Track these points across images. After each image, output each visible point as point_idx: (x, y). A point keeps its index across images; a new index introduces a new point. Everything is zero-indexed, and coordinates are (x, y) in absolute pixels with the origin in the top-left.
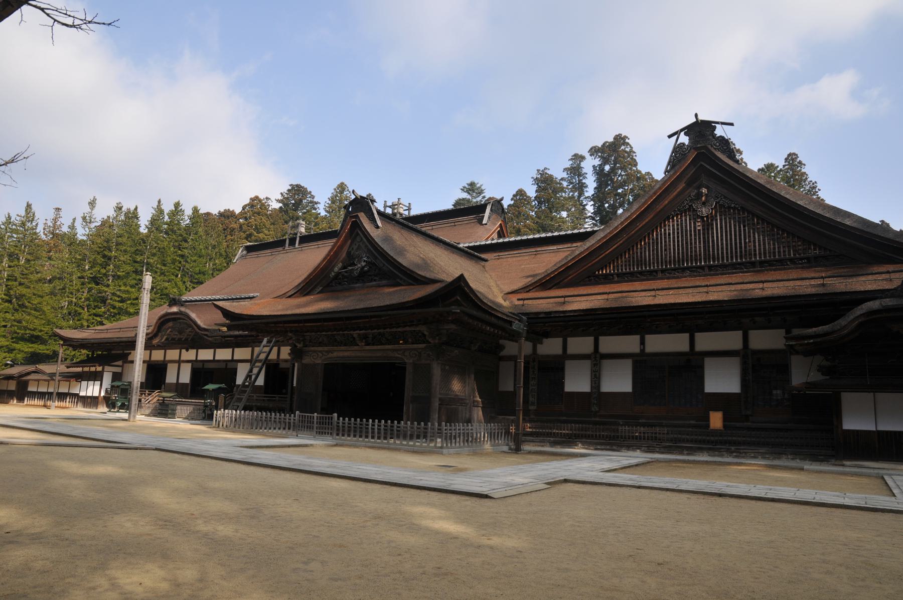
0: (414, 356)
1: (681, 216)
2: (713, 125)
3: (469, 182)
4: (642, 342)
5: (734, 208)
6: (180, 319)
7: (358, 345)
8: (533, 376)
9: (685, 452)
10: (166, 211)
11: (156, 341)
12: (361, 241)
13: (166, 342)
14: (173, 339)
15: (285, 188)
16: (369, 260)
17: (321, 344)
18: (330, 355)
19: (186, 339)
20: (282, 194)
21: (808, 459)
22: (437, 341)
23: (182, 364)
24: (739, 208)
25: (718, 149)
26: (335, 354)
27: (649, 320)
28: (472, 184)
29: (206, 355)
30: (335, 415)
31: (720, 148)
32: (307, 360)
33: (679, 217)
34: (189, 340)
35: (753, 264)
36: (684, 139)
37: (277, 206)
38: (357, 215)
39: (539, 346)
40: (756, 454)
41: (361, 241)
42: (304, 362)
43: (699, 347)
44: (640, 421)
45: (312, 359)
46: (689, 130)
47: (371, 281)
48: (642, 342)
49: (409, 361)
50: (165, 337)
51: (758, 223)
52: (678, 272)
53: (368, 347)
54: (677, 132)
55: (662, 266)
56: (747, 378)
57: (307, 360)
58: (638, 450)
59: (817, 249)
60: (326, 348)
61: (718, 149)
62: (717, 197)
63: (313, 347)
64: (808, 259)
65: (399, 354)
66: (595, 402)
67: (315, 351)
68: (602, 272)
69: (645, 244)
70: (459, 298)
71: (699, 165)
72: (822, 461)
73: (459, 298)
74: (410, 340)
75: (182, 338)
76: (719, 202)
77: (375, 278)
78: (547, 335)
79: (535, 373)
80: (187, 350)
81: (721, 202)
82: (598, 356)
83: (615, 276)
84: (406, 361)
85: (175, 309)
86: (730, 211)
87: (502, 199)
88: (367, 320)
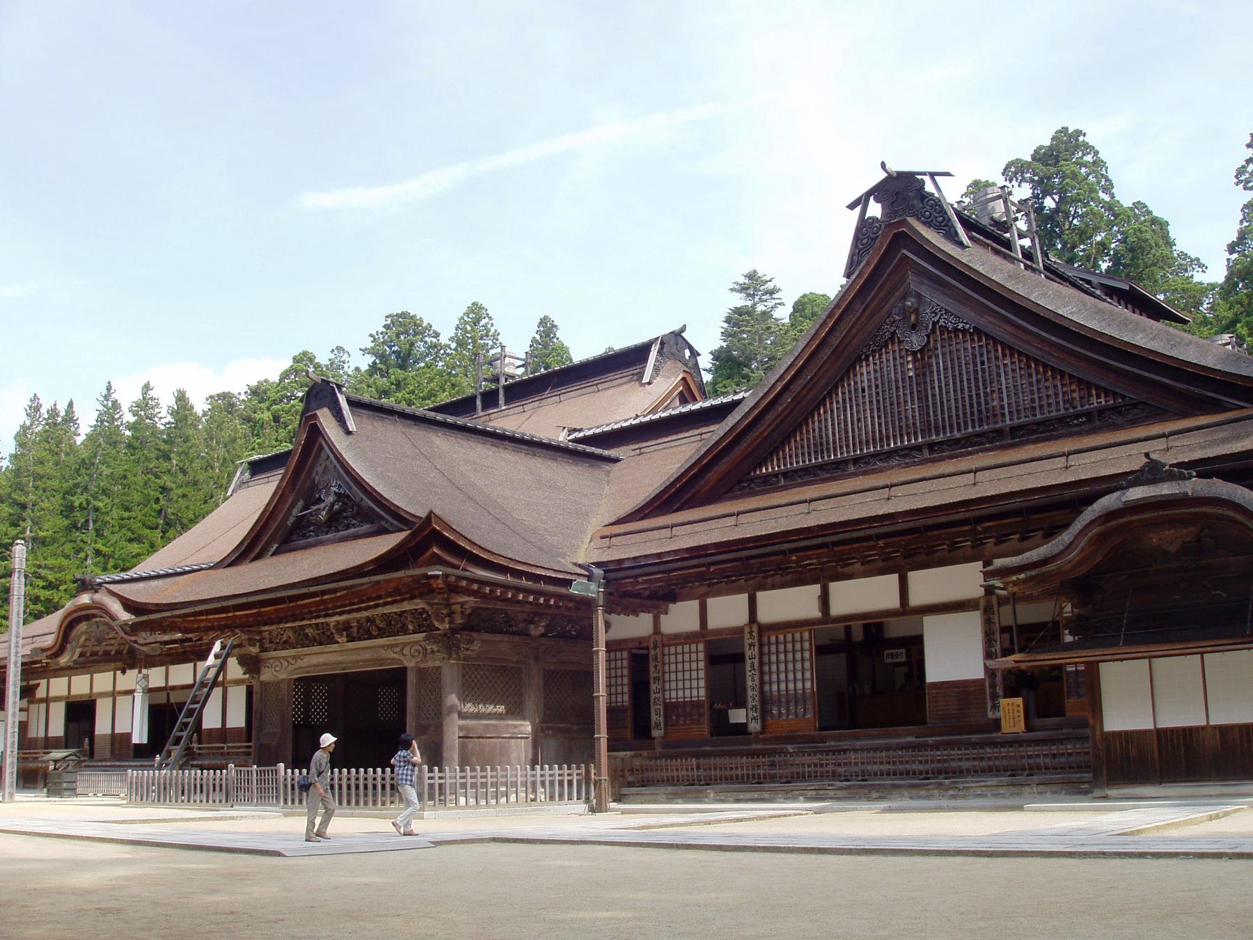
0: (417, 654)
1: (880, 355)
2: (919, 177)
3: (746, 272)
4: (824, 600)
5: (964, 331)
6: (94, 616)
7: (338, 643)
8: (656, 675)
9: (875, 795)
10: (125, 405)
11: (65, 660)
12: (327, 459)
13: (81, 660)
14: (94, 654)
15: (378, 326)
16: (342, 491)
17: (286, 645)
18: (300, 663)
19: (119, 652)
20: (371, 335)
21: (1063, 792)
22: (447, 626)
23: (119, 699)
24: (971, 331)
25: (929, 223)
26: (307, 661)
27: (794, 558)
28: (752, 276)
29: (156, 677)
30: (282, 765)
31: (932, 221)
32: (266, 675)
33: (877, 356)
34: (125, 652)
35: (999, 433)
36: (875, 210)
37: (365, 362)
38: (316, 414)
39: (662, 617)
40: (984, 789)
41: (327, 459)
42: (263, 678)
43: (915, 600)
44: (828, 744)
45: (274, 673)
46: (877, 192)
47: (348, 527)
49: (410, 664)
50: (78, 651)
51: (1004, 356)
52: (880, 460)
53: (351, 645)
54: (860, 198)
55: (854, 451)
56: (993, 650)
57: (266, 675)
58: (801, 798)
59: (1103, 395)
60: (292, 652)
61: (929, 223)
62: (934, 312)
63: (275, 650)
64: (1088, 414)
65: (395, 653)
67: (277, 658)
68: (761, 470)
69: (825, 412)
70: (436, 550)
71: (899, 256)
72: (1085, 792)
73: (436, 550)
74: (410, 627)
75: (111, 651)
76: (938, 321)
78: (673, 597)
79: (658, 668)
80: (124, 672)
81: (942, 322)
82: (755, 629)
83: (780, 476)
84: (407, 664)
85: (85, 599)
86: (957, 336)
87: (683, 329)
88: (318, 599)
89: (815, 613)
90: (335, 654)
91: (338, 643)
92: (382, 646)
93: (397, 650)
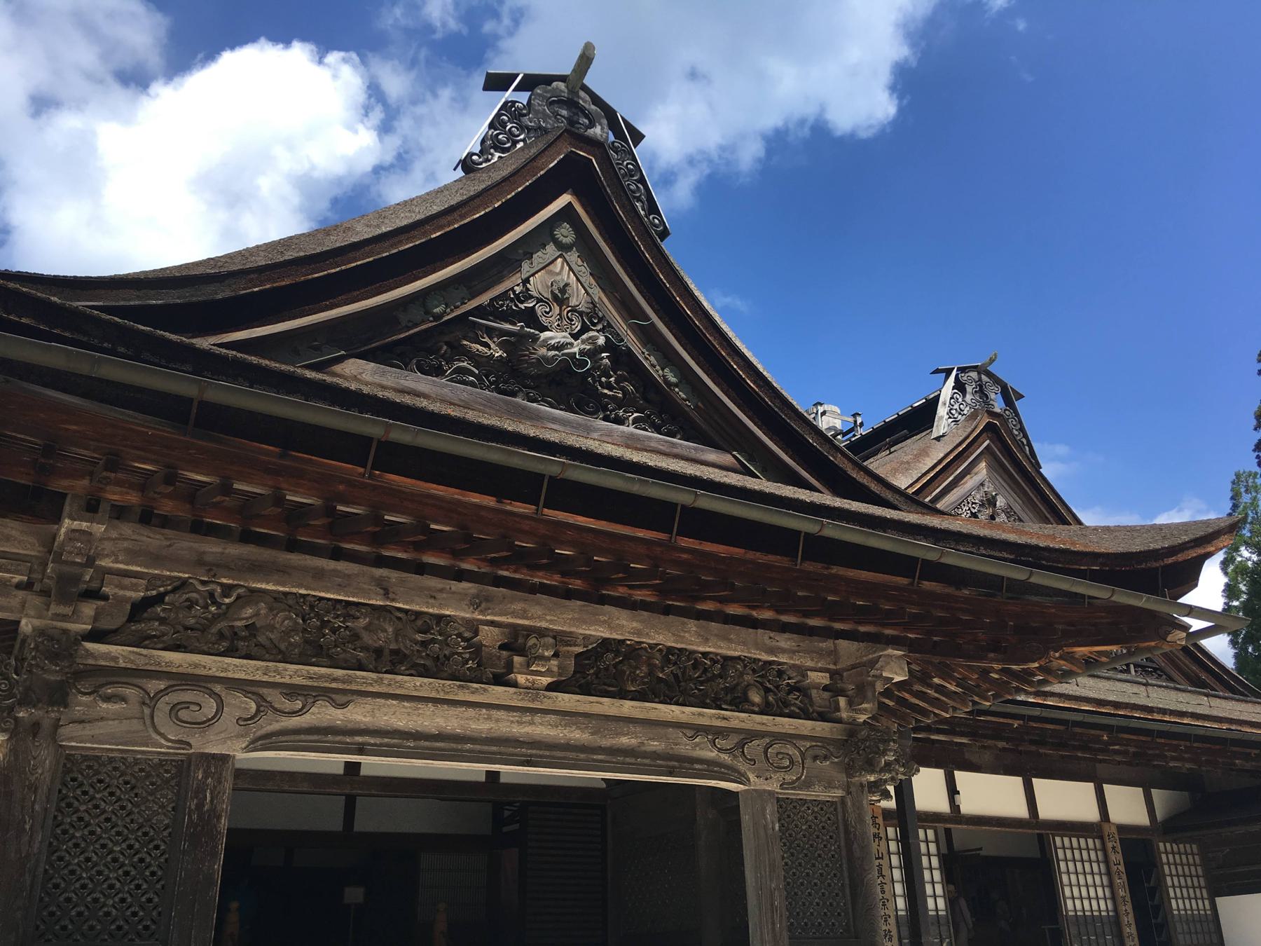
7: (514, 684)
53: (566, 701)
60: (293, 673)
65: (720, 750)
74: (756, 698)
90: (501, 714)
91: (514, 684)
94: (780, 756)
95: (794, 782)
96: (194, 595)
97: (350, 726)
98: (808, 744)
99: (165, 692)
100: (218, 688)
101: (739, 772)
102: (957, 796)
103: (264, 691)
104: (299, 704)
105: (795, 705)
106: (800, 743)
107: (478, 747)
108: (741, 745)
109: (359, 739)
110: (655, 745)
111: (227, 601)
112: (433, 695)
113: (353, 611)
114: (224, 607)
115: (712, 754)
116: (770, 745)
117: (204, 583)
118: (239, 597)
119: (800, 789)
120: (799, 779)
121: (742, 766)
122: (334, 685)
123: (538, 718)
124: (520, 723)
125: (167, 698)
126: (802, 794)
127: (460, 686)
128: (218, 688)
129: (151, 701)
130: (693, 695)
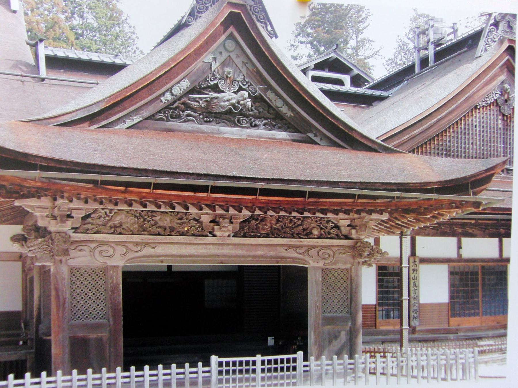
0: (327, 256)
4: (459, 247)
48: (459, 247)
60: (136, 238)
65: (299, 253)
66: (415, 315)
74: (316, 232)
77: (257, 122)
89: (453, 255)
90: (211, 246)
92: (283, 246)
93: (301, 251)
94: (324, 254)
95: (329, 263)
96: (100, 214)
97: (157, 254)
98: (337, 249)
99: (97, 247)
100: (113, 245)
101: (306, 261)
102: (460, 250)
103: (127, 245)
104: (139, 248)
105: (333, 234)
106: (332, 248)
107: (203, 259)
108: (308, 251)
109: (161, 258)
110: (271, 254)
111: (111, 215)
112: (185, 242)
113: (154, 214)
114: (110, 217)
115: (295, 255)
116: (320, 250)
117: (103, 209)
118: (115, 213)
119: (332, 265)
120: (331, 262)
121: (307, 258)
122: (150, 241)
123: (225, 247)
124: (218, 249)
125: (97, 249)
126: (334, 267)
127: (195, 238)
128: (113, 245)
129: (92, 250)
130: (289, 233)
